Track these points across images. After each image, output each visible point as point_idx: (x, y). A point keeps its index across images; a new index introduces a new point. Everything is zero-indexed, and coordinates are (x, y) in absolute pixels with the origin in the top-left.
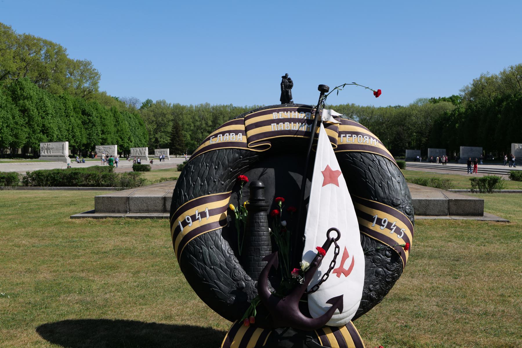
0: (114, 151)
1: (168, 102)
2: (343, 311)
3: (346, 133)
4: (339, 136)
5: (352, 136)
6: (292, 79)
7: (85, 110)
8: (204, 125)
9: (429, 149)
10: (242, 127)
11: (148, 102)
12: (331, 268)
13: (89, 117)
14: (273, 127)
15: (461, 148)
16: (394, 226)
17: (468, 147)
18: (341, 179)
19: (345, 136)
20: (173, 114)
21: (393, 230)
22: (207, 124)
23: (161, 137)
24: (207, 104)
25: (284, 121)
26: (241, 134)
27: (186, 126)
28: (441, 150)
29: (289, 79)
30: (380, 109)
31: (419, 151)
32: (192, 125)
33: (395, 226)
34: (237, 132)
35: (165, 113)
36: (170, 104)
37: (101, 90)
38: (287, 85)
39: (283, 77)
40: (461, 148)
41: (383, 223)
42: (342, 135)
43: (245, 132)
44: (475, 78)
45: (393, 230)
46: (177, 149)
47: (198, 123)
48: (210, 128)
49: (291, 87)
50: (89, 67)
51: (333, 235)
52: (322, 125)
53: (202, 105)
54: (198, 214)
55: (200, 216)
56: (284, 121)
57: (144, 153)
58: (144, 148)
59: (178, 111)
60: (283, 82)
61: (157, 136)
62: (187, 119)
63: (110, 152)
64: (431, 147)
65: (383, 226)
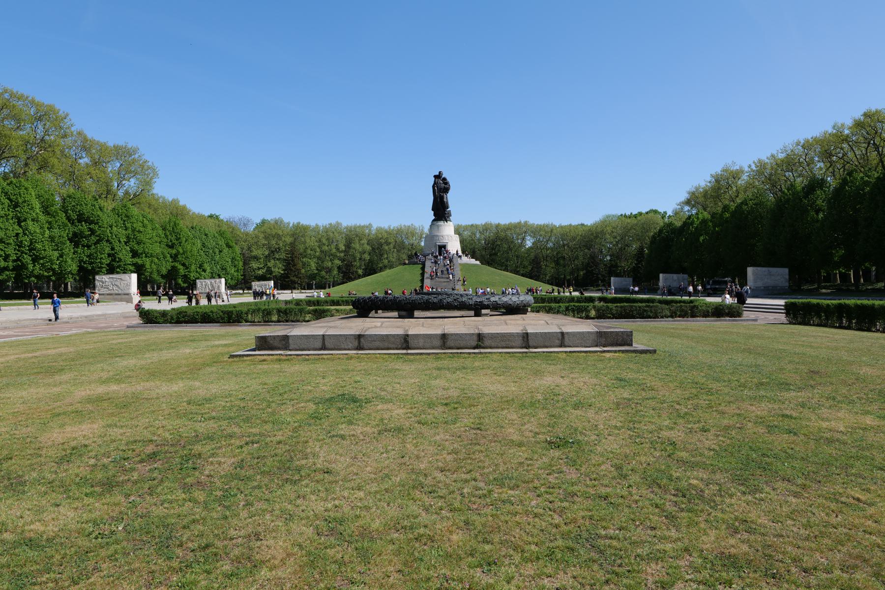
0: (129, 285)
1: (286, 220)
6: (449, 179)
7: (84, 214)
8: (334, 250)
9: (661, 275)
11: (264, 222)
13: (92, 226)
15: (750, 270)
17: (764, 269)
20: (293, 235)
22: (338, 249)
23: (275, 266)
24: (338, 224)
27: (309, 252)
28: (681, 275)
29: (445, 179)
30: (561, 227)
31: (631, 279)
32: (318, 250)
35: (281, 233)
36: (289, 224)
37: (155, 191)
38: (441, 187)
39: (435, 177)
40: (750, 270)
44: (713, 173)
46: (294, 282)
47: (326, 248)
48: (342, 255)
49: (446, 190)
50: (136, 156)
53: (330, 224)
57: (219, 287)
58: (218, 280)
59: (299, 232)
60: (435, 183)
61: (270, 264)
62: (311, 242)
63: (121, 287)
64: (663, 272)
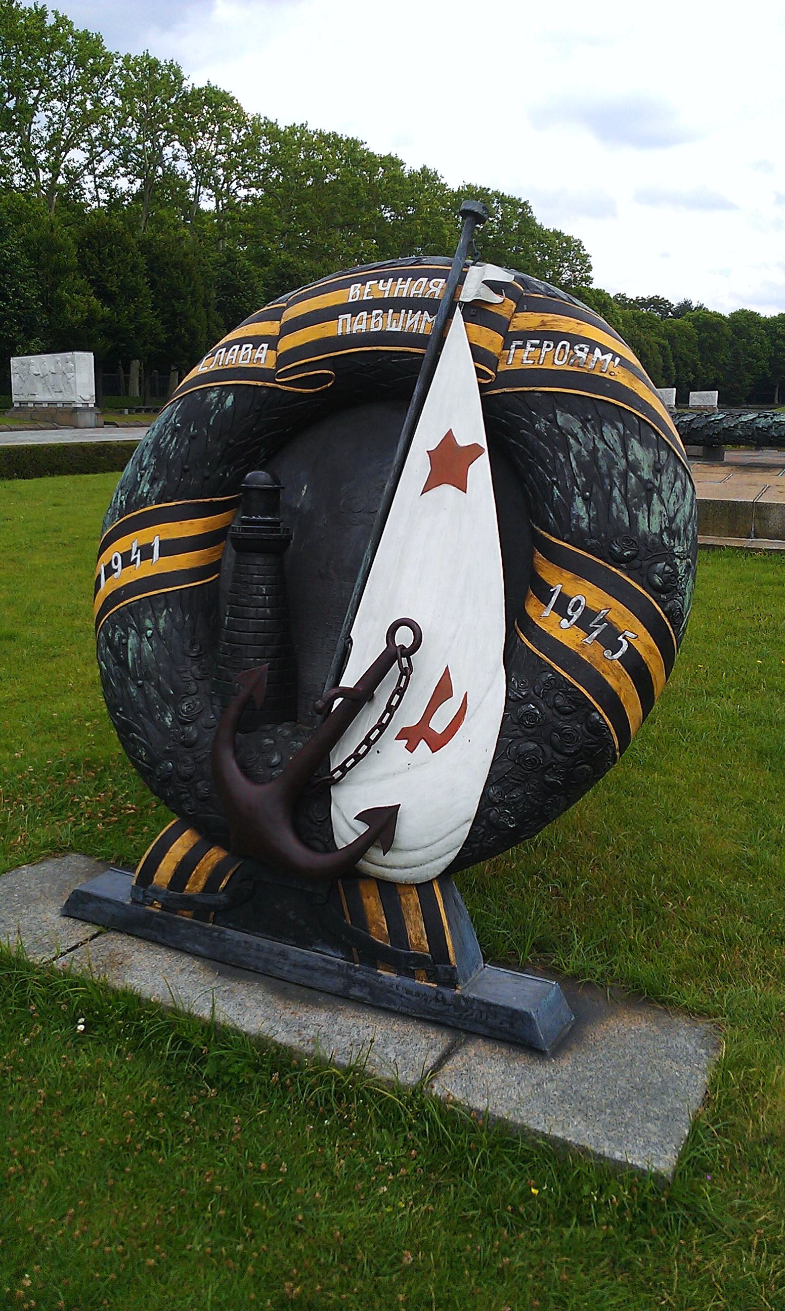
2: (395, 845)
3: (525, 336)
4: (506, 347)
5: (540, 346)
10: (271, 328)
12: (381, 727)
14: (346, 325)
16: (600, 622)
18: (481, 472)
19: (523, 347)
21: (595, 634)
25: (368, 306)
26: (265, 346)
33: (600, 622)
34: (256, 341)
41: (570, 613)
42: (516, 343)
43: (273, 342)
45: (595, 634)
51: (404, 637)
52: (458, 315)
54: (138, 549)
55: (138, 556)
56: (368, 306)
65: (569, 618)
